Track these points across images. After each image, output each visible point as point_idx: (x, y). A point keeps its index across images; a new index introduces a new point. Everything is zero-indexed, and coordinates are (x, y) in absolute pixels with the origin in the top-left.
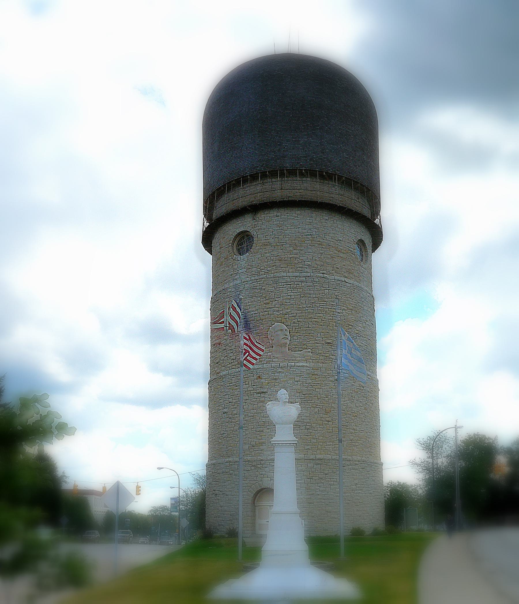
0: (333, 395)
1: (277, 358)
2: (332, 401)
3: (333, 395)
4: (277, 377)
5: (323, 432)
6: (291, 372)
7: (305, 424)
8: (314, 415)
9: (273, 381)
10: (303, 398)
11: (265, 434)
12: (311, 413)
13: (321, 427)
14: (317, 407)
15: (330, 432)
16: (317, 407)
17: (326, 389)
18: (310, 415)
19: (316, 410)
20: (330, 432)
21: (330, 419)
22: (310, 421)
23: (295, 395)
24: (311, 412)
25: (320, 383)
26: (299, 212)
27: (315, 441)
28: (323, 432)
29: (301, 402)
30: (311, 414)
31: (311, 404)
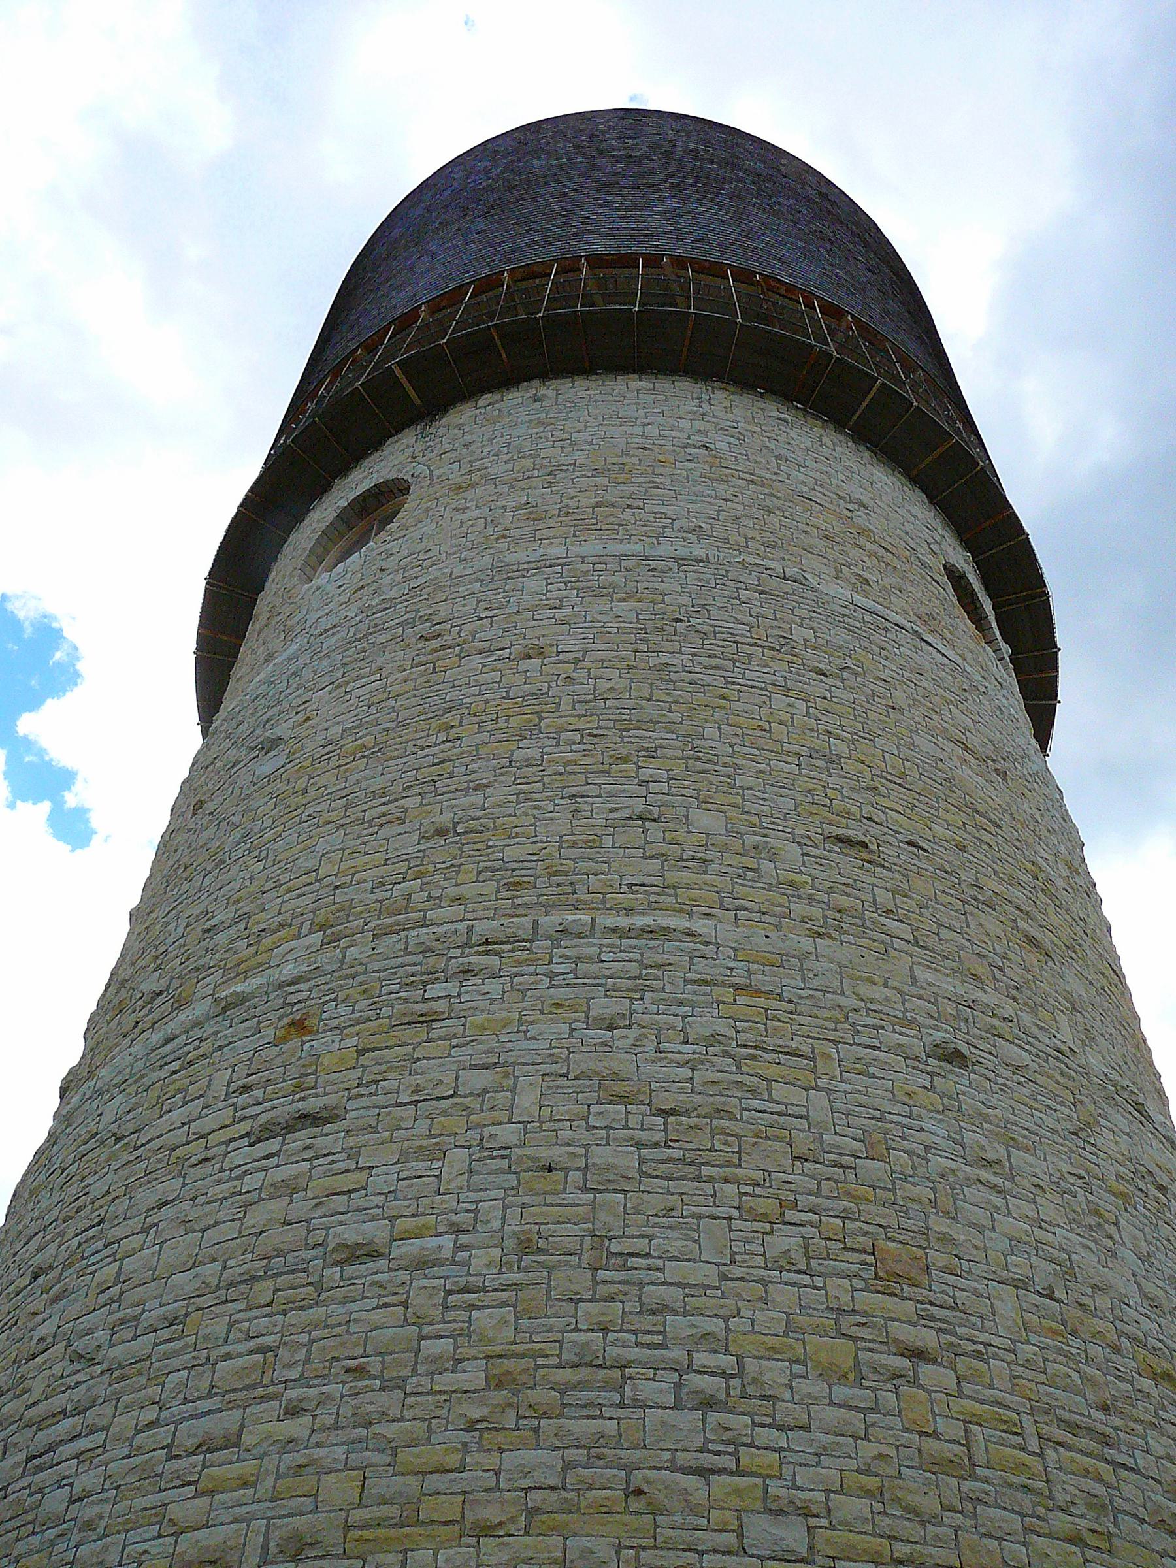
0: (927, 1148)
1: (458, 899)
2: (923, 1191)
3: (927, 1148)
4: (441, 1006)
5: (868, 1450)
6: (561, 968)
7: (676, 1353)
8: (762, 1281)
9: (407, 1033)
10: (660, 1136)
11: (248, 1467)
12: (733, 1262)
13: (842, 1392)
14: (790, 1215)
15: (939, 1466)
16: (790, 1215)
17: (862, 1099)
18: (724, 1277)
19: (785, 1241)
20: (939, 1466)
21: (927, 1338)
22: (728, 1330)
23: (585, 1119)
24: (733, 1254)
25: (805, 1049)
26: (645, 384)
27: (793, 1535)
28: (868, 1450)
29: (643, 1174)
30: (737, 1272)
31: (730, 1189)
